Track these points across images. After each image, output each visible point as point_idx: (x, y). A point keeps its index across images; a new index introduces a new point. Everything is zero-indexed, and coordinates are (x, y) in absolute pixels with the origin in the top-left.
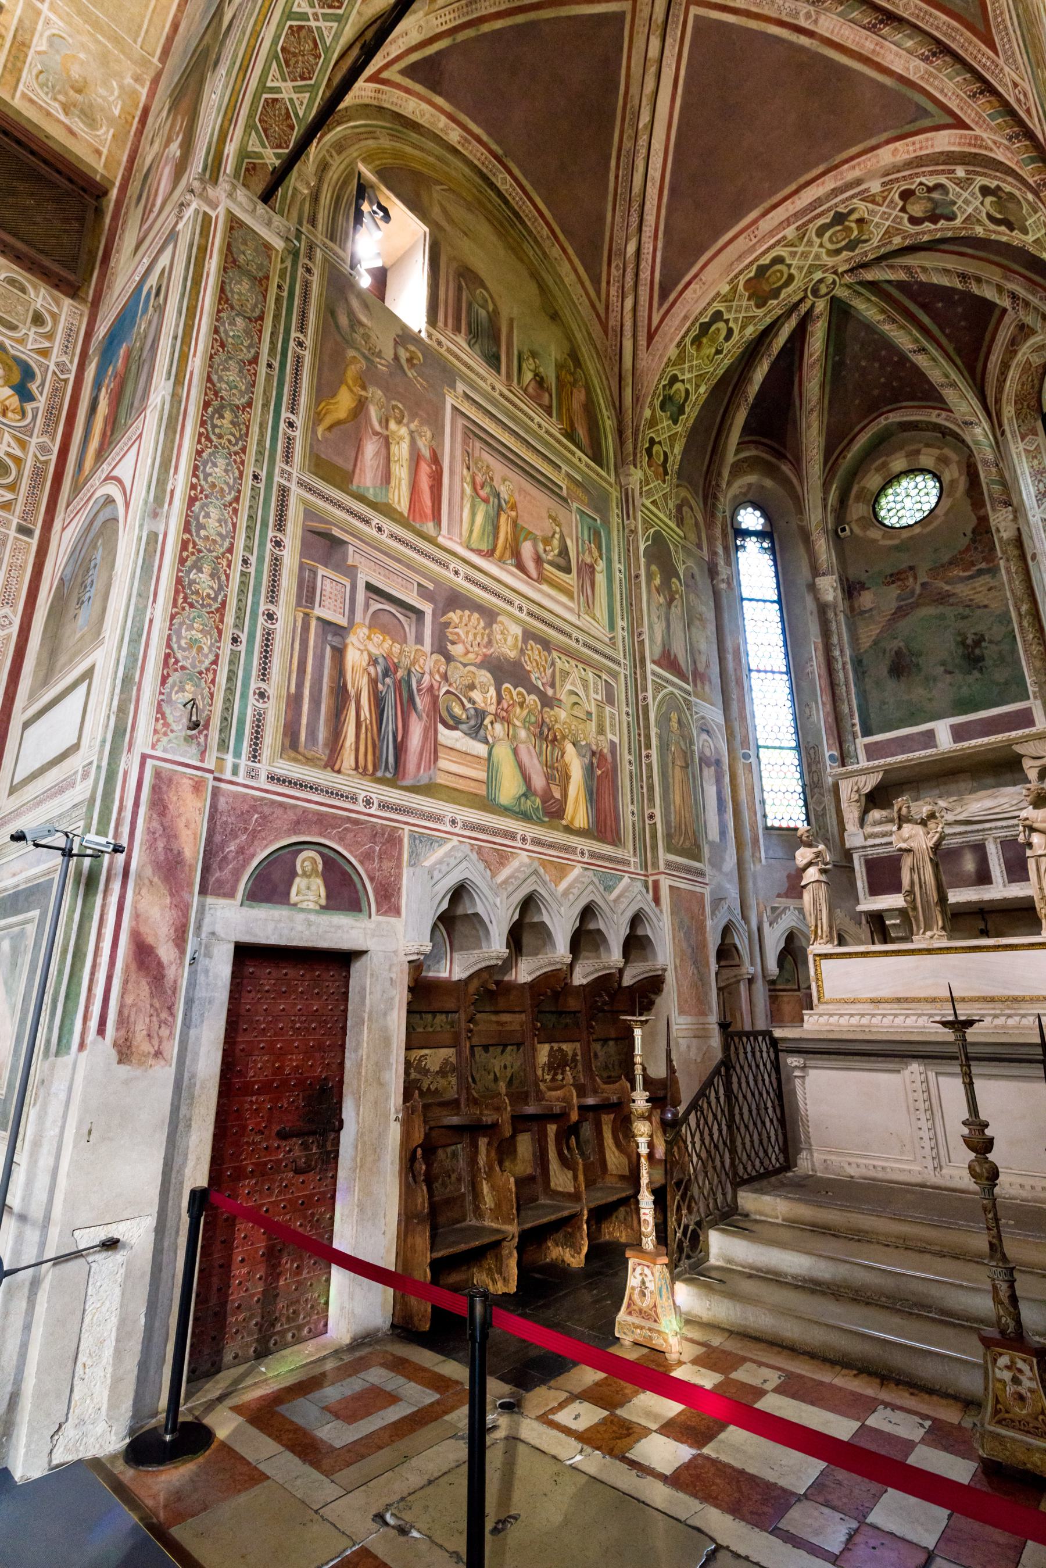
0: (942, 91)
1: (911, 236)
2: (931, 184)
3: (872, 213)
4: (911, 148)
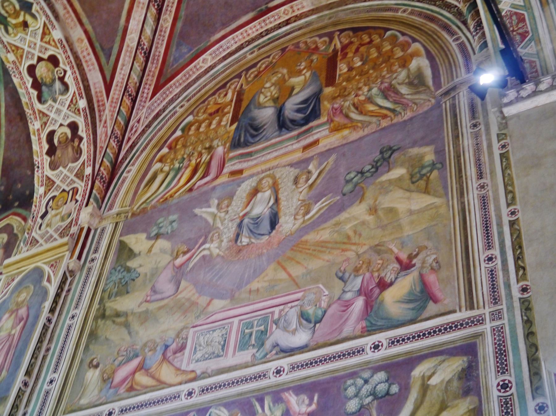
0: (123, 65)
1: (17, 68)
2: (66, 79)
3: (34, 33)
4: (85, 53)
